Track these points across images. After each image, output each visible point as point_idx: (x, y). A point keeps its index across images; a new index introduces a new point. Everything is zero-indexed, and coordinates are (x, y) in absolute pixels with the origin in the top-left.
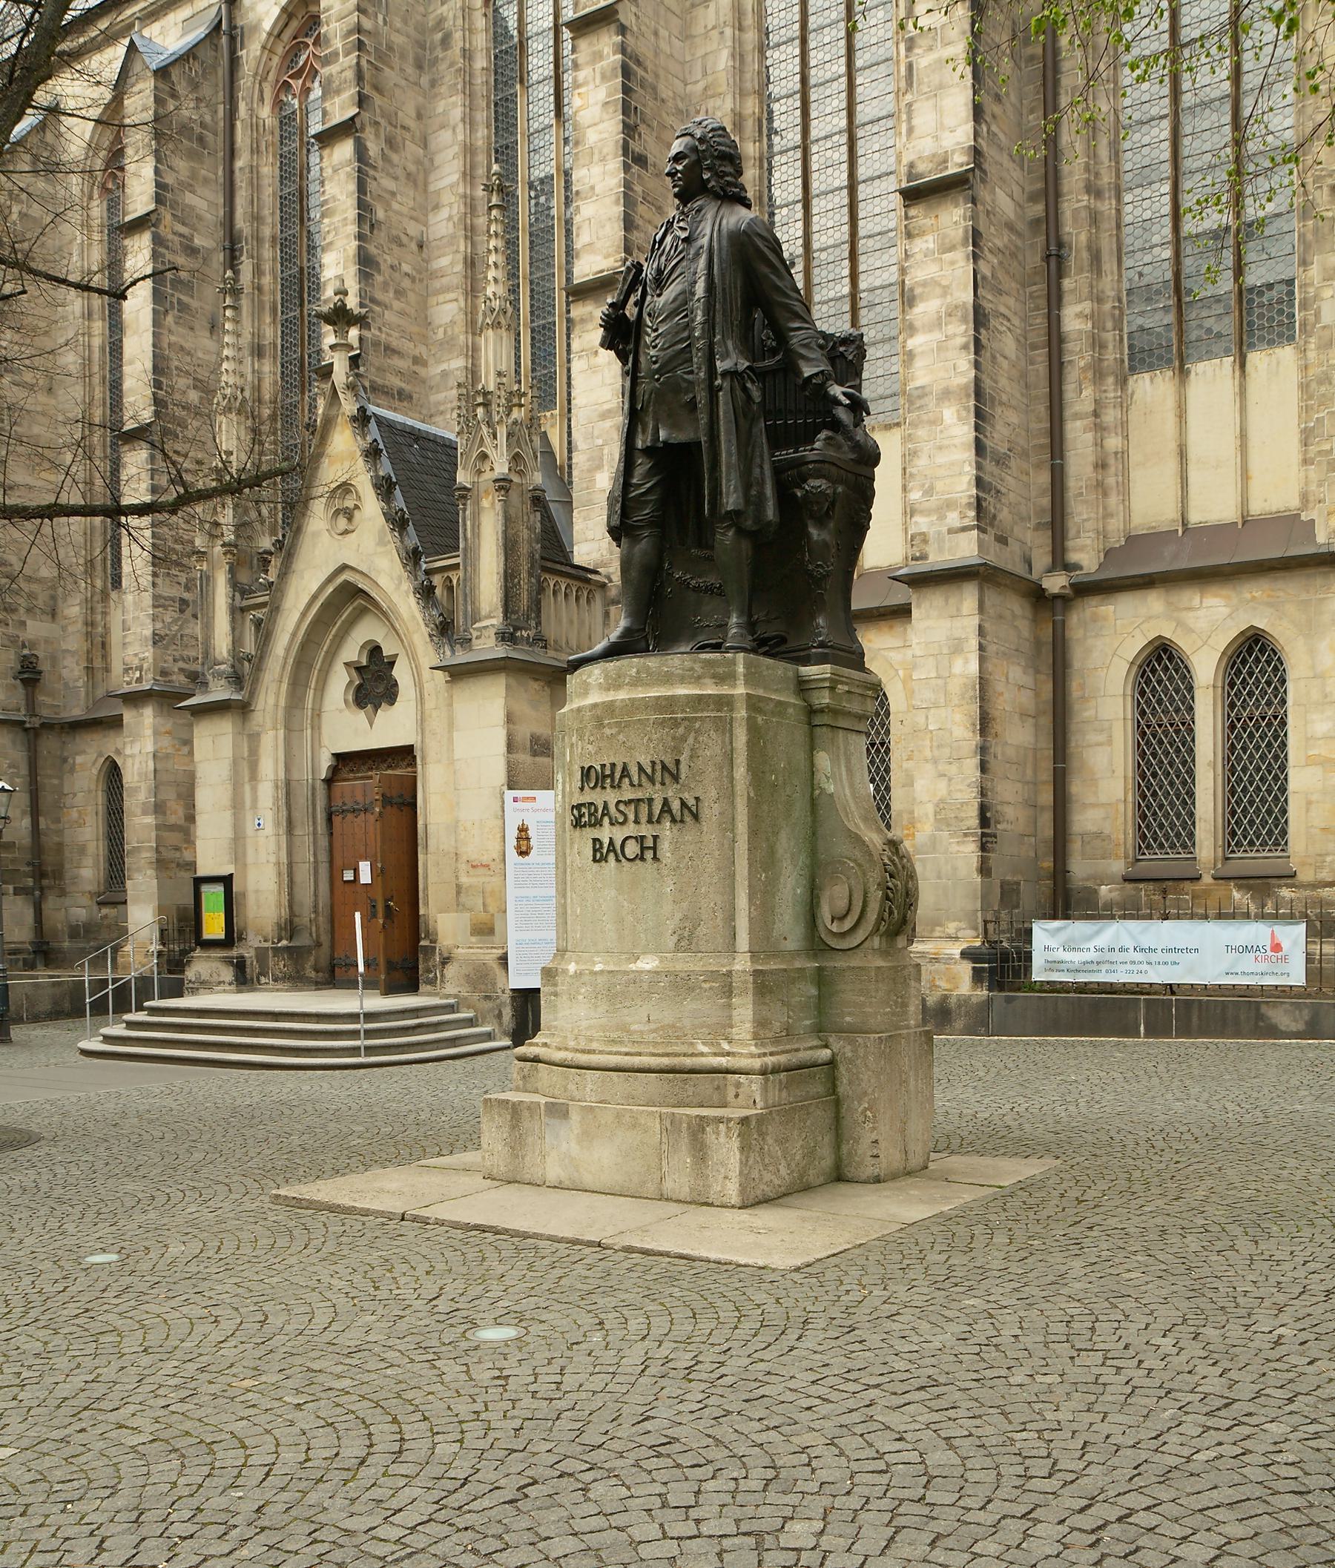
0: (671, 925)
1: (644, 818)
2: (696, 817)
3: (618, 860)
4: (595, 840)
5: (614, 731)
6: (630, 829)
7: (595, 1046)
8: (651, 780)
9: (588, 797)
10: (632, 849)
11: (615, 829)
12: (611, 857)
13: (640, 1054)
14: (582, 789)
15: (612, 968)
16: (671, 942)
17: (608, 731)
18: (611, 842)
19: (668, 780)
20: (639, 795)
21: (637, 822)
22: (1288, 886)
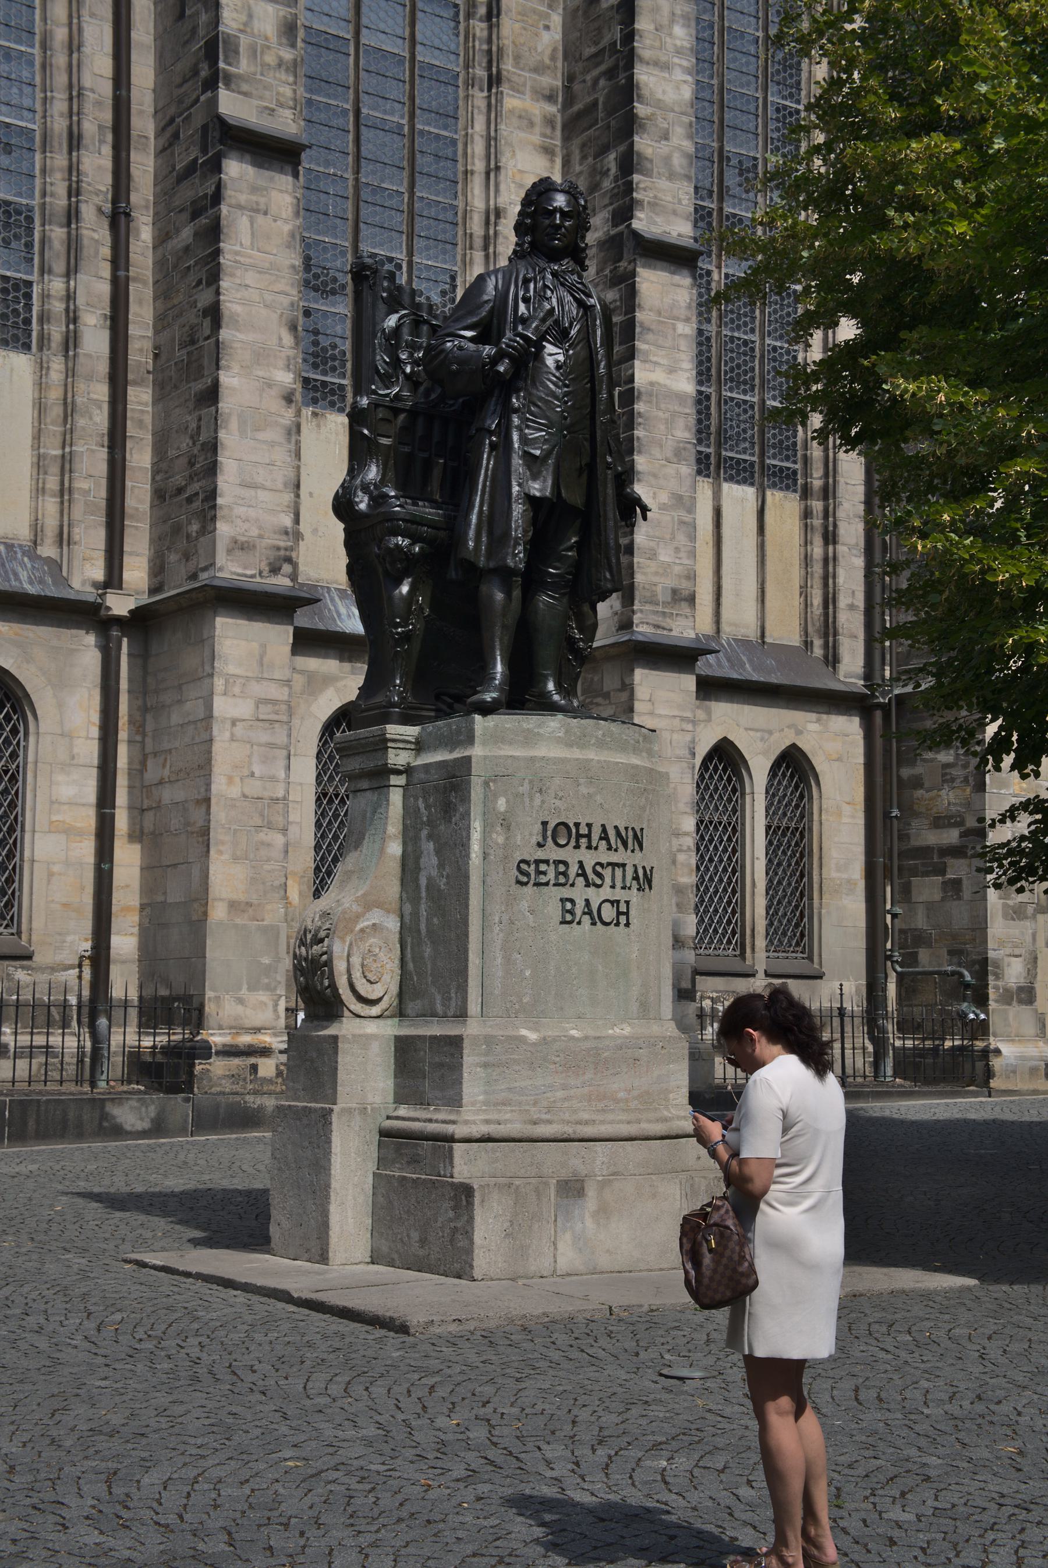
0: (635, 992)
1: (619, 884)
2: (650, 888)
3: (594, 924)
4: (563, 901)
5: (592, 790)
6: (606, 892)
7: (586, 1116)
8: (625, 844)
9: (552, 853)
10: (608, 912)
11: (591, 890)
12: (586, 919)
13: (639, 1121)
14: (540, 845)
15: (591, 1033)
16: (634, 1007)
17: (584, 790)
18: (587, 901)
19: (637, 847)
20: (615, 858)
21: (613, 887)
22: (28, 968)
